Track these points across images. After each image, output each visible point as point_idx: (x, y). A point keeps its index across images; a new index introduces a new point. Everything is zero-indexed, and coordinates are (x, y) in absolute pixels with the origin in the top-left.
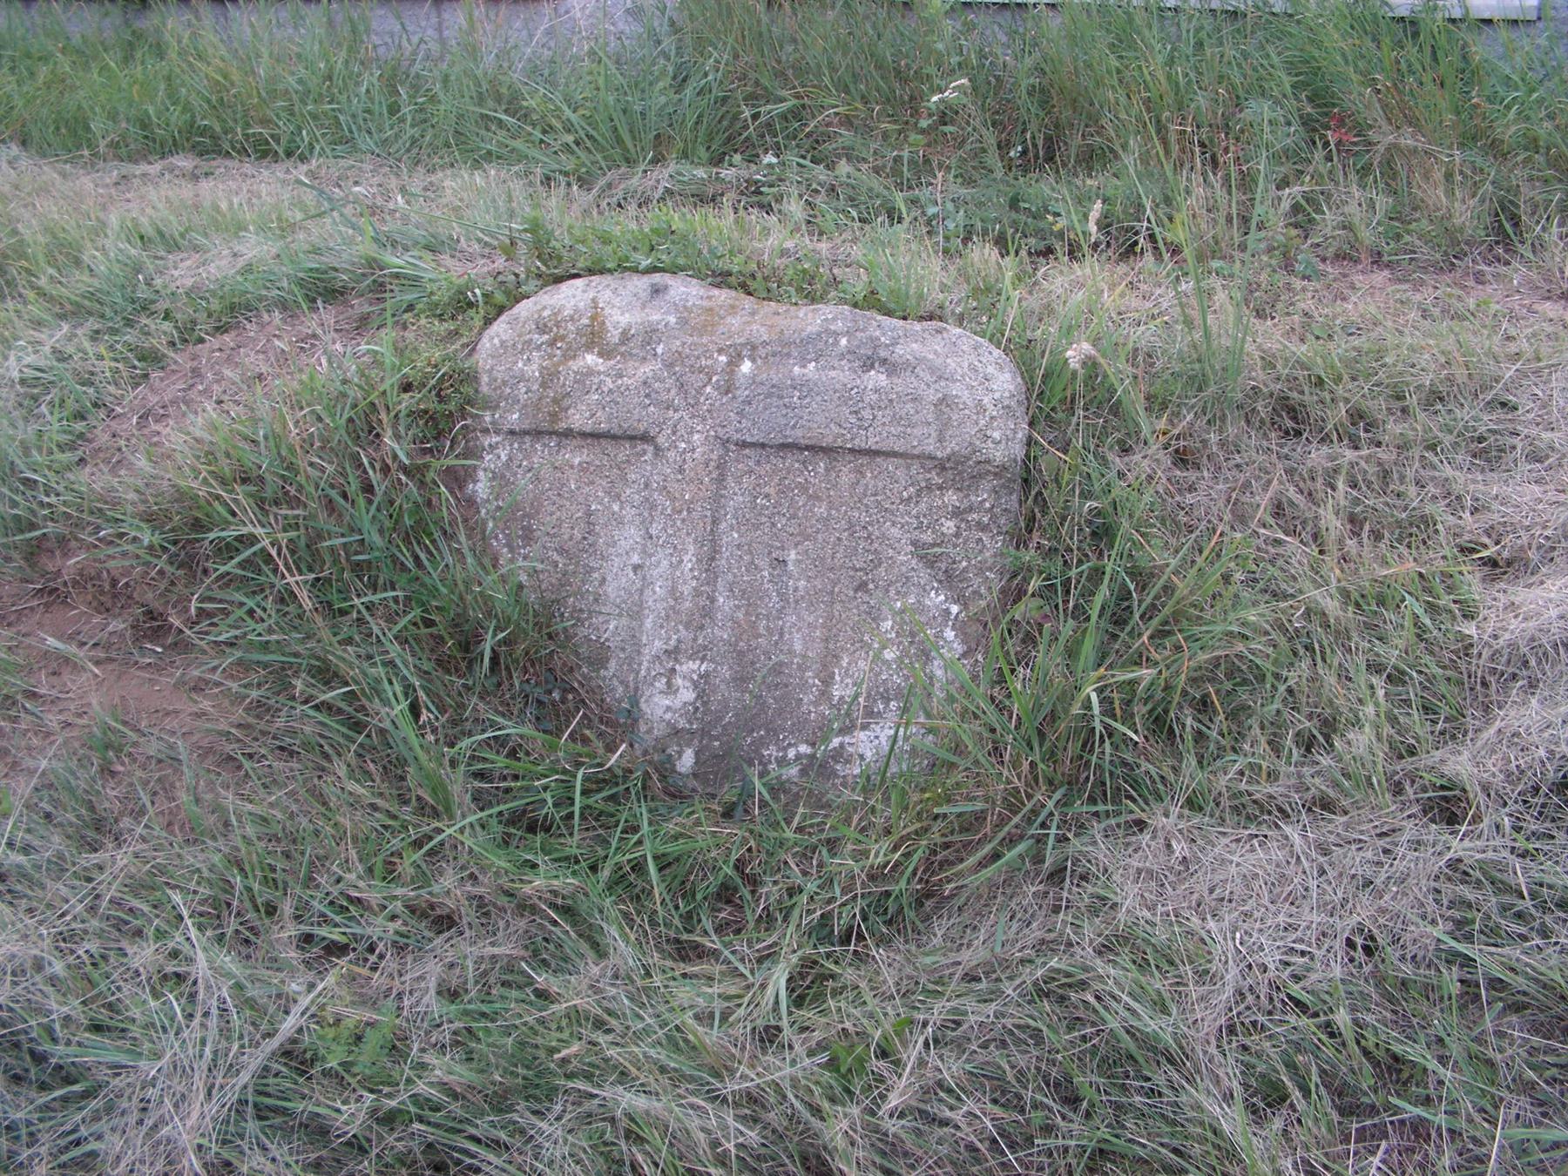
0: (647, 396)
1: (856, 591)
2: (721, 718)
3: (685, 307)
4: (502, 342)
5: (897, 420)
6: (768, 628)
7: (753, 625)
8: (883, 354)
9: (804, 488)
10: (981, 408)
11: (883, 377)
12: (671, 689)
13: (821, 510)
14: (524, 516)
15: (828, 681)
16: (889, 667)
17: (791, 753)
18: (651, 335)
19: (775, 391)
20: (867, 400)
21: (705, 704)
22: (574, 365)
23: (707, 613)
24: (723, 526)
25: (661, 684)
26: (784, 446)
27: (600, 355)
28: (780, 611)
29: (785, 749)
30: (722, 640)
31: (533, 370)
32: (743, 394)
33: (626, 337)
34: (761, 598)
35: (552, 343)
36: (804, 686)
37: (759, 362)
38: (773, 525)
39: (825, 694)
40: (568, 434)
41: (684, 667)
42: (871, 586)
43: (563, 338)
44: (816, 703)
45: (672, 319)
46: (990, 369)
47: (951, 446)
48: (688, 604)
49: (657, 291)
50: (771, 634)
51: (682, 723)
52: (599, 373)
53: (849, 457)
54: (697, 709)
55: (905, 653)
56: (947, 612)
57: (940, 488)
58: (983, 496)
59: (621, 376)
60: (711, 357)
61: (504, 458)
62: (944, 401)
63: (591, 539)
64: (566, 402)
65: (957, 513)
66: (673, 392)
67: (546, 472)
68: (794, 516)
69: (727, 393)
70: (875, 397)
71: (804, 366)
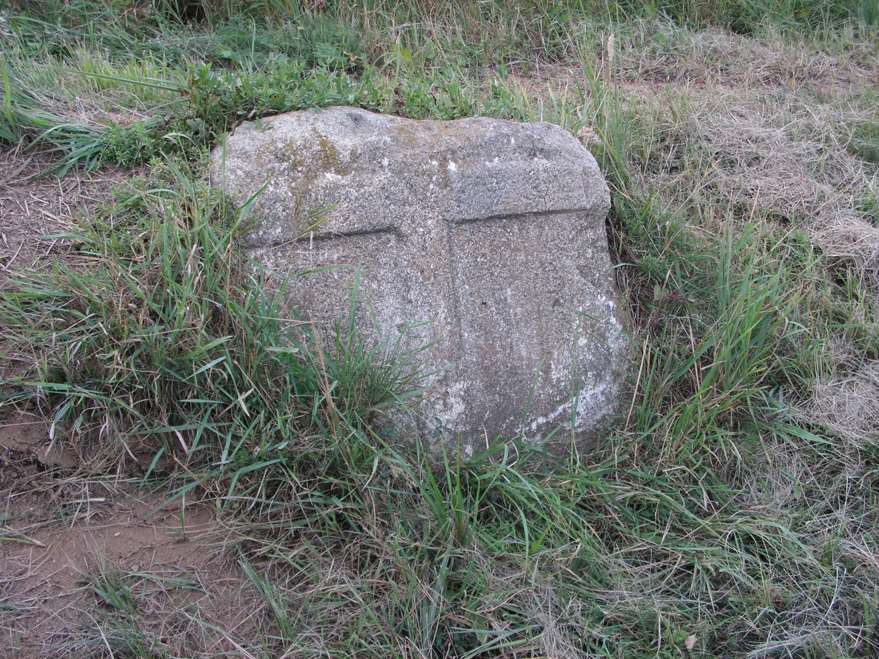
0: (387, 197)
1: (553, 306)
2: (482, 418)
5: (562, 188)
6: (502, 346)
7: (492, 346)
9: (507, 245)
13: (521, 257)
14: (300, 308)
15: (547, 370)
16: (583, 351)
17: (534, 426)
18: (374, 153)
19: (479, 181)
20: (541, 178)
23: (460, 346)
24: (458, 281)
25: (439, 406)
27: (338, 172)
28: (508, 333)
29: (529, 424)
30: (473, 362)
31: (284, 190)
34: (493, 327)
35: (294, 167)
36: (533, 377)
37: (460, 162)
38: (492, 274)
39: (547, 380)
40: (328, 236)
41: (454, 388)
42: (562, 301)
43: (301, 163)
44: (543, 388)
48: (447, 343)
50: (504, 349)
55: (590, 340)
59: (362, 186)
63: (360, 314)
66: (406, 192)
70: (545, 175)
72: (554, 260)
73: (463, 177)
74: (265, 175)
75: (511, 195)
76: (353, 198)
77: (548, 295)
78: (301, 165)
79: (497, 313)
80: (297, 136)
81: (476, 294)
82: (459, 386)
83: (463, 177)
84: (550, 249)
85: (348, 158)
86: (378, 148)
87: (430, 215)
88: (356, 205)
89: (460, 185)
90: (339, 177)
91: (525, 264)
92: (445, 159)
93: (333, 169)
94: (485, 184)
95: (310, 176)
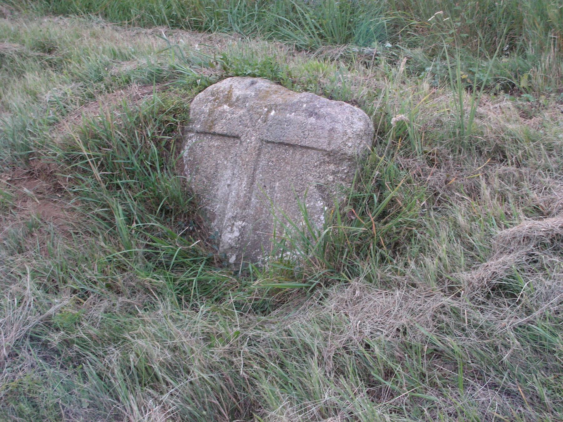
0: (240, 121)
3: (259, 90)
4: (200, 99)
5: (315, 136)
6: (266, 211)
8: (316, 111)
10: (345, 133)
11: (314, 119)
12: (232, 231)
13: (288, 168)
18: (245, 99)
19: (280, 122)
20: (307, 127)
21: (242, 238)
22: (220, 109)
24: (258, 172)
25: (229, 229)
26: (280, 143)
27: (229, 106)
31: (207, 110)
32: (269, 123)
33: (238, 99)
35: (215, 100)
37: (277, 111)
38: (273, 172)
40: (214, 134)
45: (253, 94)
46: (355, 120)
47: (333, 147)
48: (242, 200)
49: (253, 83)
51: (233, 244)
52: (227, 112)
53: (300, 149)
54: (239, 239)
56: (323, 209)
57: (328, 163)
58: (344, 167)
59: (233, 114)
60: (262, 108)
61: (194, 142)
62: (332, 130)
64: (214, 123)
65: (334, 173)
66: (248, 121)
67: (206, 148)
68: (280, 170)
69: (265, 122)
70: (310, 126)
71: (291, 114)
72: (303, 174)
75: (291, 133)
82: (240, 223)
86: (247, 98)
91: (289, 172)
92: (271, 108)
94: (281, 125)
95: (220, 105)
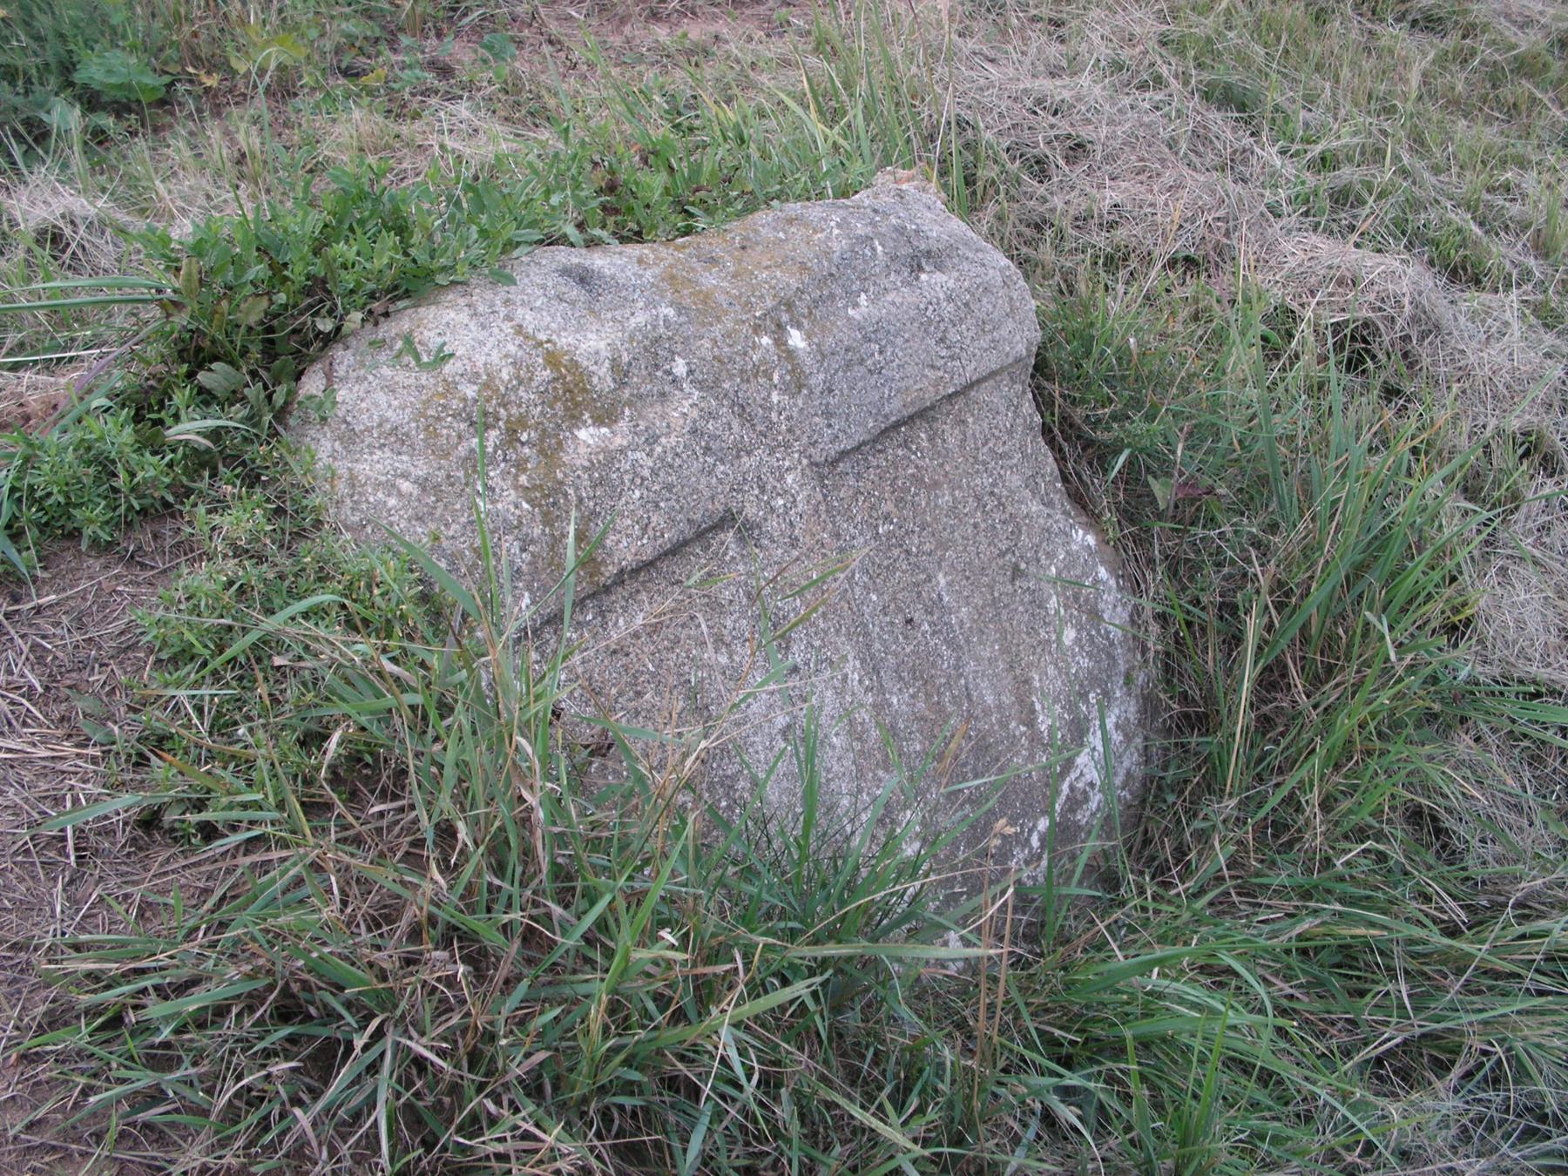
0: (707, 450)
1: (1013, 580)
9: (917, 480)
15: (1031, 723)
17: (1035, 842)
18: (655, 350)
27: (599, 421)
31: (510, 502)
32: (817, 380)
33: (621, 373)
34: (934, 664)
36: (1014, 741)
38: (908, 552)
42: (1023, 566)
43: (522, 422)
53: (946, 408)
59: (653, 440)
72: (994, 485)
73: (824, 356)
74: (461, 474)
75: (909, 369)
76: (646, 473)
77: (1001, 562)
78: (525, 427)
79: (934, 633)
80: (495, 357)
81: (892, 606)
83: (824, 356)
84: (985, 463)
85: (609, 379)
86: (657, 340)
87: (787, 463)
88: (657, 487)
89: (821, 376)
90: (604, 430)
92: (779, 326)
93: (586, 416)
94: (862, 362)
95: (550, 450)
